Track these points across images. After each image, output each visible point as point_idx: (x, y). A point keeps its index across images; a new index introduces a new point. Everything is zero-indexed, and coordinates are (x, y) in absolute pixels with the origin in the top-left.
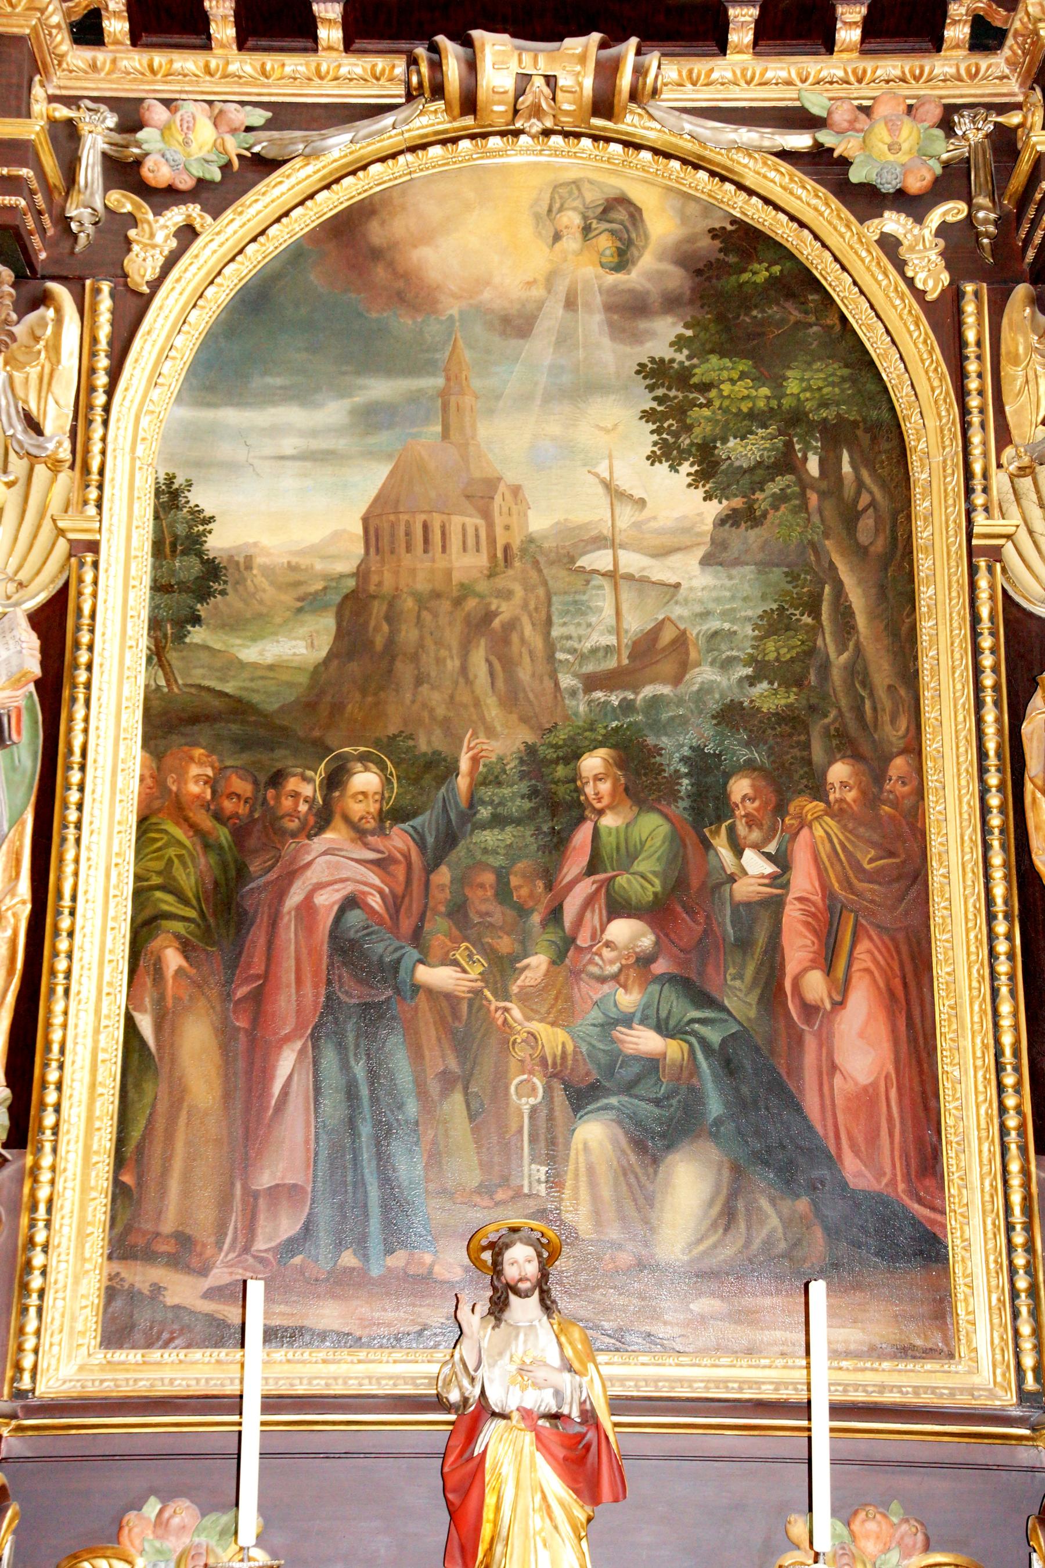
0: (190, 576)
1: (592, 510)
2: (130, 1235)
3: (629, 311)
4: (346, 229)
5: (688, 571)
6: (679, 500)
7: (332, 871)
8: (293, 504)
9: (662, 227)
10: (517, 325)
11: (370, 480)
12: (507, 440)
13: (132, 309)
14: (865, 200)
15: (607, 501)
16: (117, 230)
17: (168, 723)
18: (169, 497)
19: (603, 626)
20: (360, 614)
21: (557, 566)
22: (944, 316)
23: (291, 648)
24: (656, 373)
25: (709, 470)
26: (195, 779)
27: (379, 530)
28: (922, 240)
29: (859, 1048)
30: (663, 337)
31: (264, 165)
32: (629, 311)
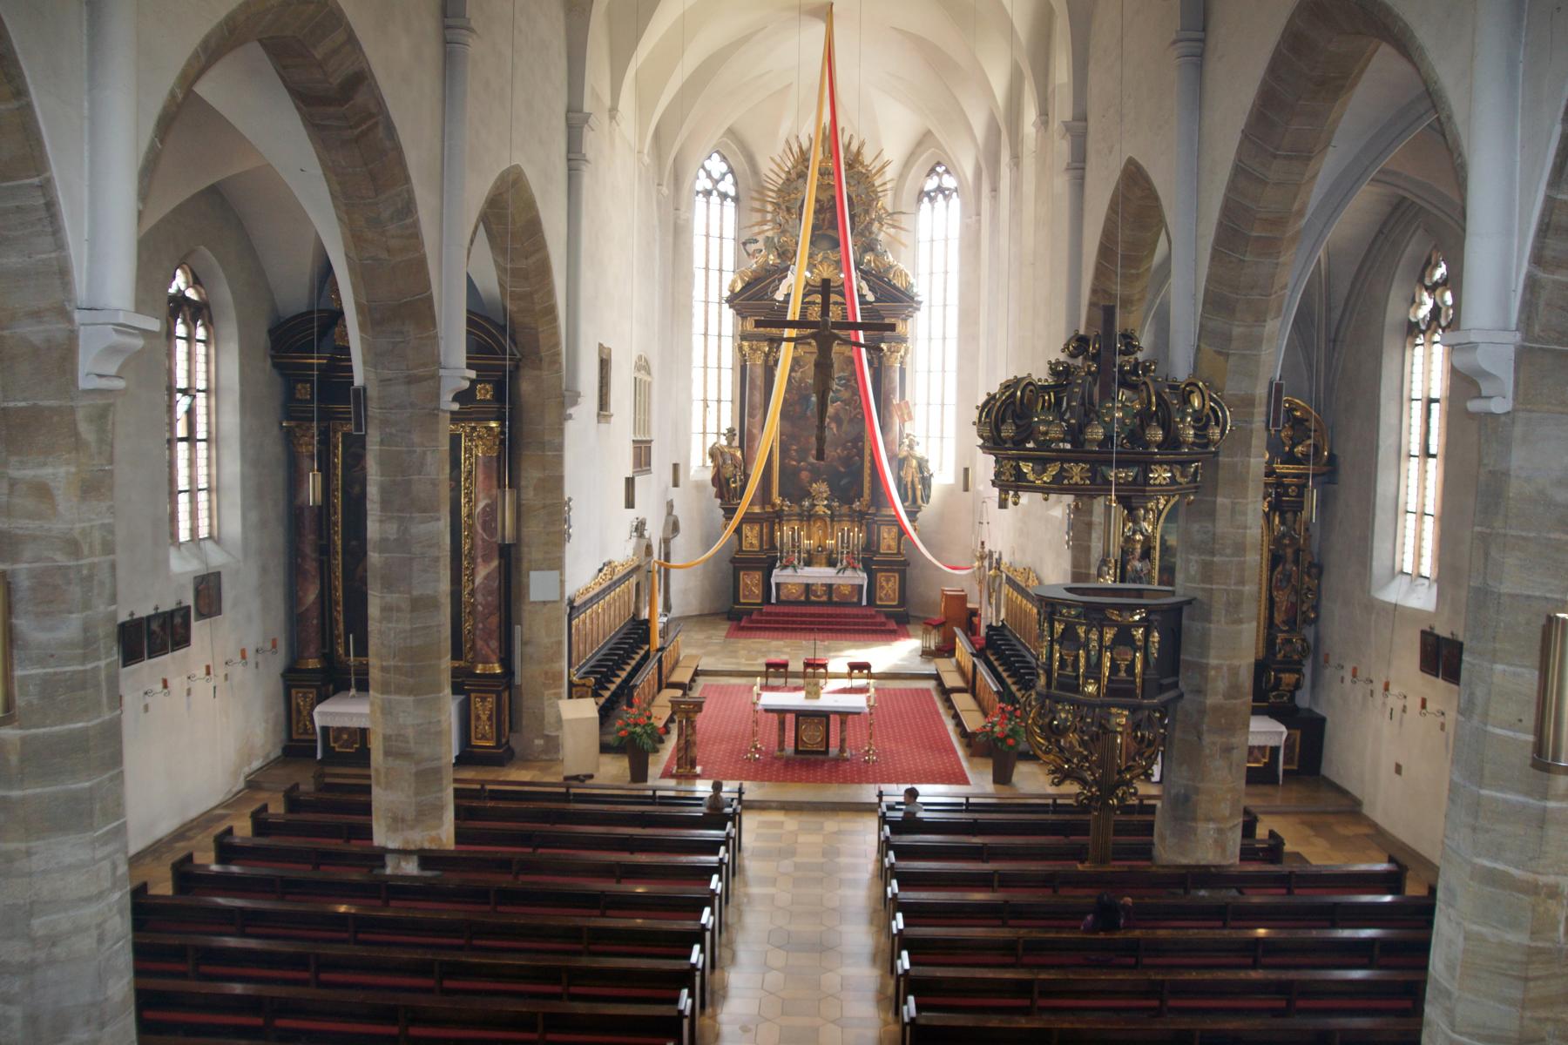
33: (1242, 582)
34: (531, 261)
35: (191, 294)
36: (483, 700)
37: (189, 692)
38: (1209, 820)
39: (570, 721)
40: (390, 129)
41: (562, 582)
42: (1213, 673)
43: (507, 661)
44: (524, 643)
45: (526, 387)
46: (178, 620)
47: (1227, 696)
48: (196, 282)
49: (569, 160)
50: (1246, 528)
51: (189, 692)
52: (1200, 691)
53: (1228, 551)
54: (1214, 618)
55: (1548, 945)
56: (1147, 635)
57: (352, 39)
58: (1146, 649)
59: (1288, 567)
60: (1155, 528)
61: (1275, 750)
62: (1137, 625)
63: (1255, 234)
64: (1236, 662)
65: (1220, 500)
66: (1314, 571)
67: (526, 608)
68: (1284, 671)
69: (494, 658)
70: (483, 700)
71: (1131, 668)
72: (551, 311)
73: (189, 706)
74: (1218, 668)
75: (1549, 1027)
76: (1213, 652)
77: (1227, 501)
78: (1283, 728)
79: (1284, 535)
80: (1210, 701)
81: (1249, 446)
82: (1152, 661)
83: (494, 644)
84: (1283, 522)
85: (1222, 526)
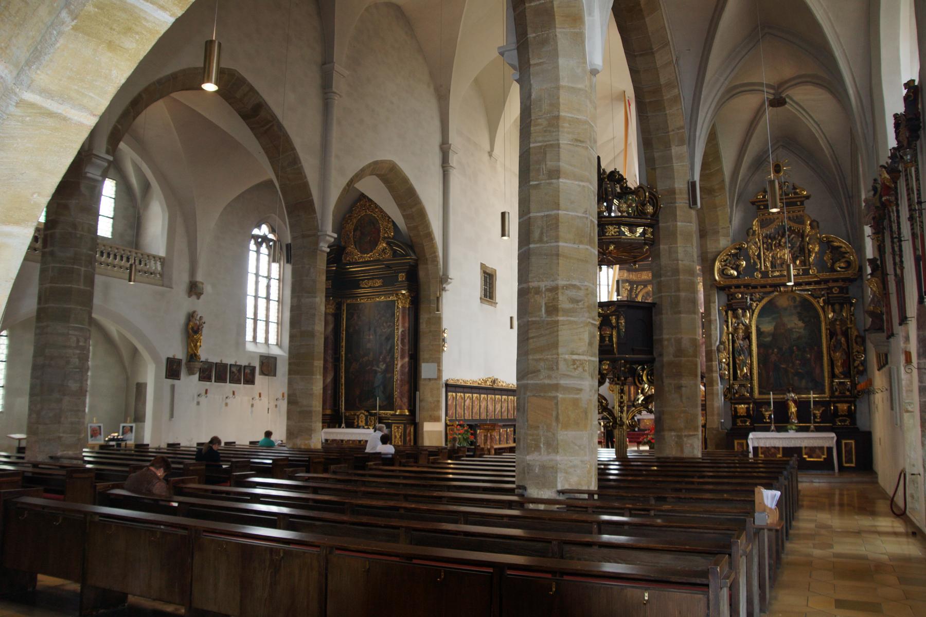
0: (759, 333)
1: (793, 325)
2: (760, 386)
3: (795, 307)
4: (770, 301)
5: (802, 331)
6: (801, 324)
7: (773, 358)
8: (768, 328)
9: (798, 299)
10: (786, 309)
11: (774, 324)
12: (785, 320)
13: (753, 312)
14: (816, 298)
15: (795, 324)
16: (751, 304)
17: (759, 346)
18: (757, 327)
19: (795, 336)
20: (774, 335)
21: (791, 330)
22: (823, 308)
23: (768, 339)
24: (798, 313)
25: (804, 322)
26: (762, 351)
27: (776, 328)
28: (821, 300)
29: (818, 371)
30: (799, 309)
31: (763, 298)
32: (795, 307)
33: (678, 290)
34: (414, 210)
35: (271, 236)
36: (398, 427)
37: (252, 406)
38: (671, 430)
39: (427, 432)
40: (280, 127)
41: (440, 371)
42: (666, 343)
43: (413, 412)
44: (420, 401)
45: (421, 274)
46: (248, 371)
47: (676, 356)
48: (273, 230)
49: (443, 167)
50: (677, 260)
51: (252, 406)
52: (661, 355)
53: (669, 274)
54: (664, 312)
55: (538, 319)
56: (618, 319)
57: (252, 89)
58: (617, 327)
59: (839, 337)
60: (750, 321)
61: (830, 449)
62: (612, 314)
63: (647, 100)
64: (679, 336)
65: (661, 247)
66: (859, 340)
67: (422, 382)
68: (839, 402)
69: (405, 407)
70: (398, 427)
71: (611, 336)
72: (429, 236)
73: (252, 412)
74: (669, 340)
75: (542, 364)
76: (665, 331)
77: (666, 247)
78: (833, 435)
79: (836, 320)
80: (665, 359)
81: (676, 215)
82: (622, 334)
83: (405, 400)
84: (834, 311)
85: (664, 260)
